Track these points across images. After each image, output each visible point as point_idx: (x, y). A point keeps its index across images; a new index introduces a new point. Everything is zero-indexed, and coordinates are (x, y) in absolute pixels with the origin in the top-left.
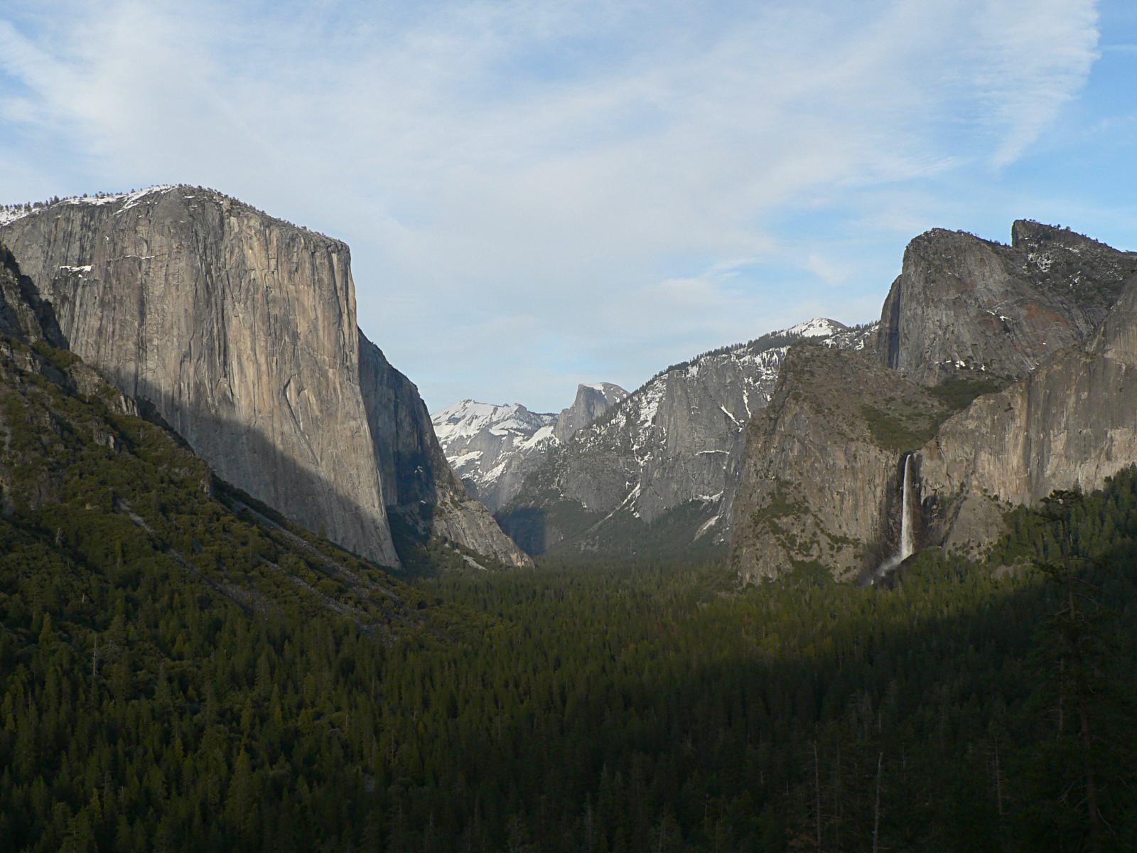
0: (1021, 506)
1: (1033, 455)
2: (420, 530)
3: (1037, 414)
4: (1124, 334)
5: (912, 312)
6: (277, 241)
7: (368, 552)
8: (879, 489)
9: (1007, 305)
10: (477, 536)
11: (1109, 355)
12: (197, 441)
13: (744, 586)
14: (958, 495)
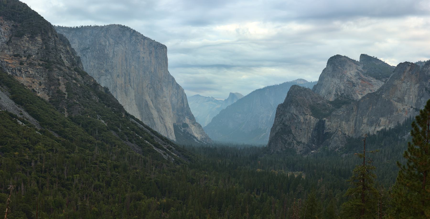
0: (352, 137)
1: (358, 123)
2: (182, 131)
3: (360, 111)
4: (388, 90)
5: (328, 79)
7: (167, 135)
8: (312, 129)
9: (355, 79)
10: (198, 133)
11: (383, 96)
12: (121, 100)
13: (271, 153)
14: (335, 132)
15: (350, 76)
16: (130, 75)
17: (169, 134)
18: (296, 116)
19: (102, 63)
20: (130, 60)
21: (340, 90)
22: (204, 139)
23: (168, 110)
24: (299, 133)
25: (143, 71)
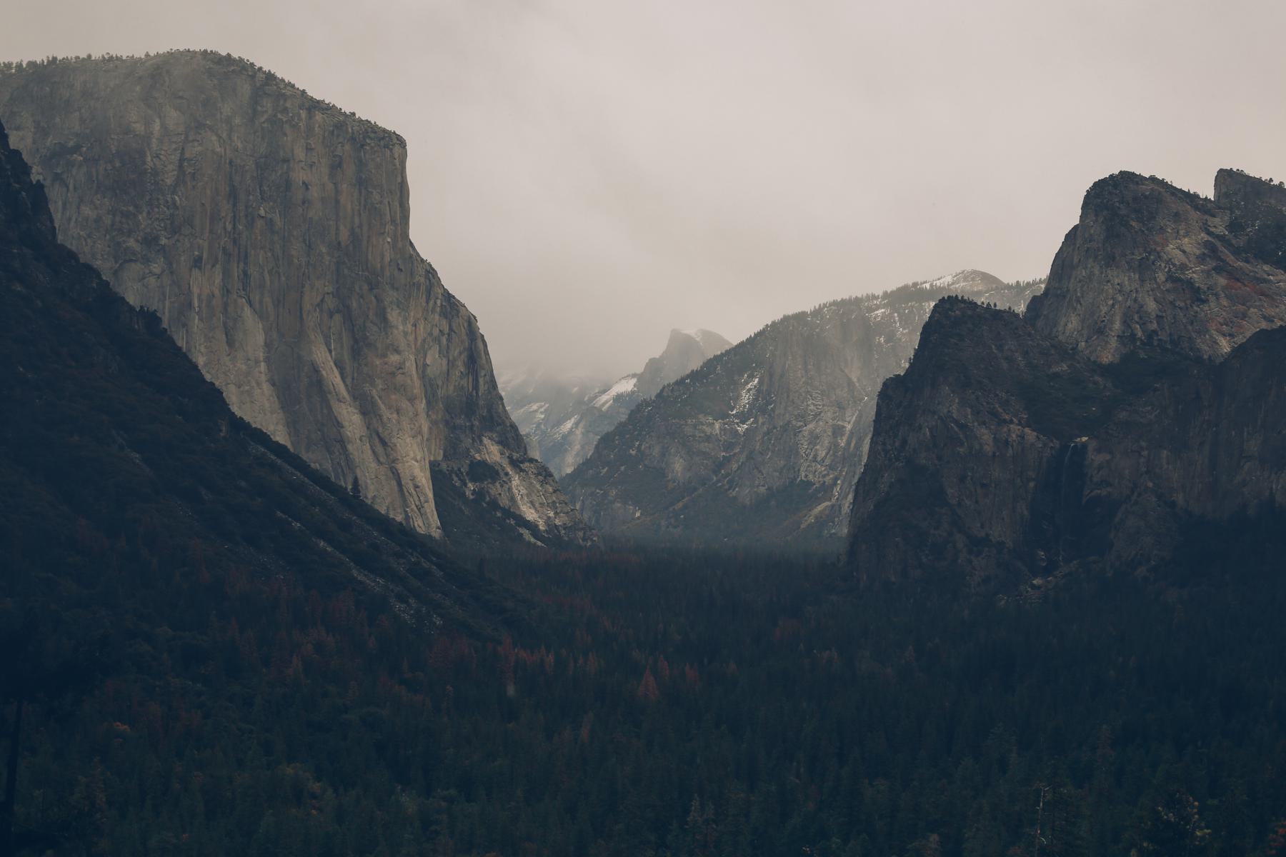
6: (319, 126)
7: (403, 516)
8: (1032, 484)
12: (206, 365)
15: (1179, 257)
16: (246, 257)
17: (412, 510)
18: (962, 427)
19: (131, 208)
20: (251, 197)
21: (1141, 318)
22: (564, 529)
23: (409, 405)
24: (977, 502)
25: (304, 241)
